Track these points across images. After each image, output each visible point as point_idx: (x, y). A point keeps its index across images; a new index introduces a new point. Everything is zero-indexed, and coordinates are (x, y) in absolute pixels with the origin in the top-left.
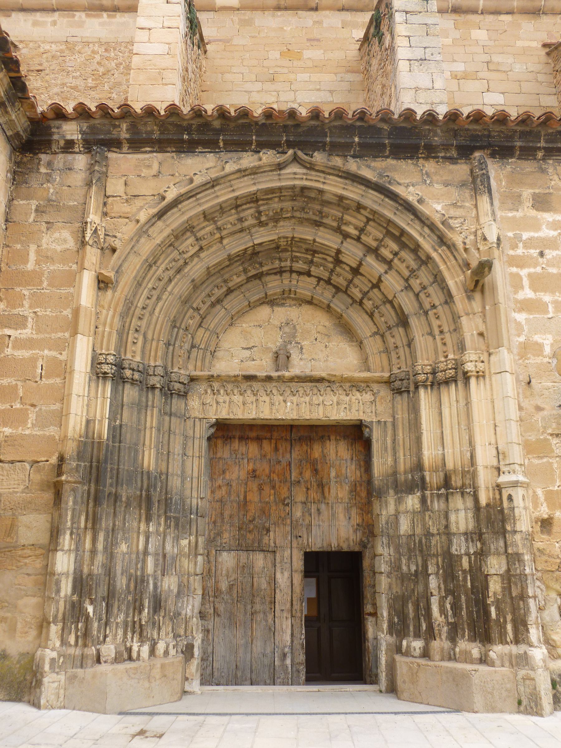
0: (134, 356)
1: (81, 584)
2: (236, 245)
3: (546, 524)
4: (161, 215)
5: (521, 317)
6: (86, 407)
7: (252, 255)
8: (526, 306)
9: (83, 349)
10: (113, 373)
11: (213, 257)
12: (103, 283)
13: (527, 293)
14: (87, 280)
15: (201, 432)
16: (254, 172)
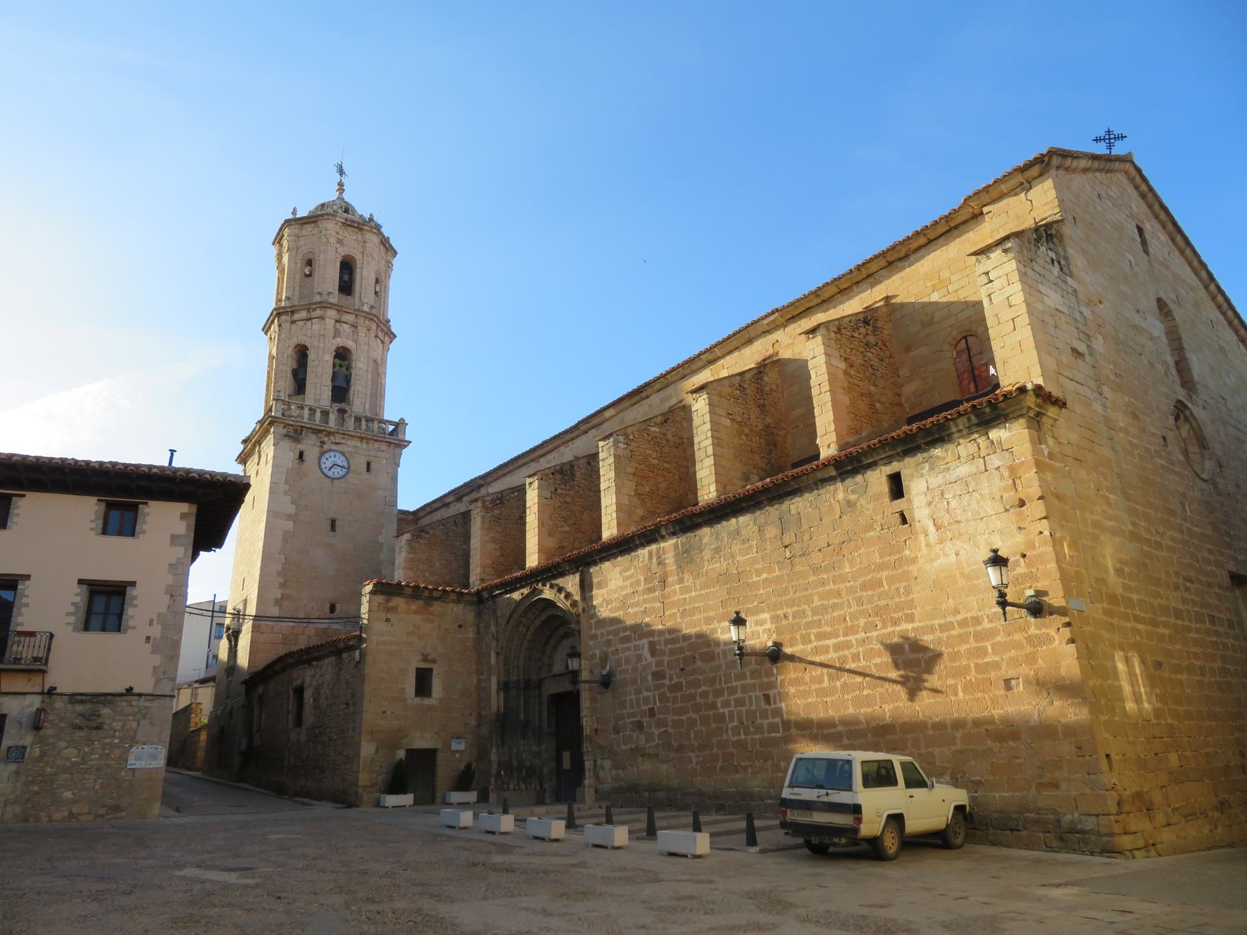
0: (514, 678)
1: (500, 764)
2: (538, 622)
3: (596, 730)
4: (508, 622)
5: (592, 643)
6: (496, 701)
7: (545, 623)
8: (594, 637)
9: (494, 680)
10: (505, 686)
11: (532, 629)
12: (498, 654)
13: (594, 631)
14: (493, 655)
15: (545, 700)
16: (528, 596)
